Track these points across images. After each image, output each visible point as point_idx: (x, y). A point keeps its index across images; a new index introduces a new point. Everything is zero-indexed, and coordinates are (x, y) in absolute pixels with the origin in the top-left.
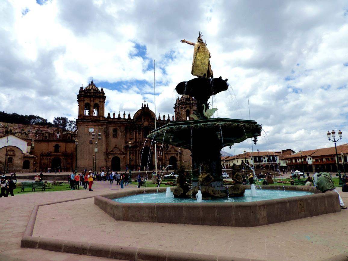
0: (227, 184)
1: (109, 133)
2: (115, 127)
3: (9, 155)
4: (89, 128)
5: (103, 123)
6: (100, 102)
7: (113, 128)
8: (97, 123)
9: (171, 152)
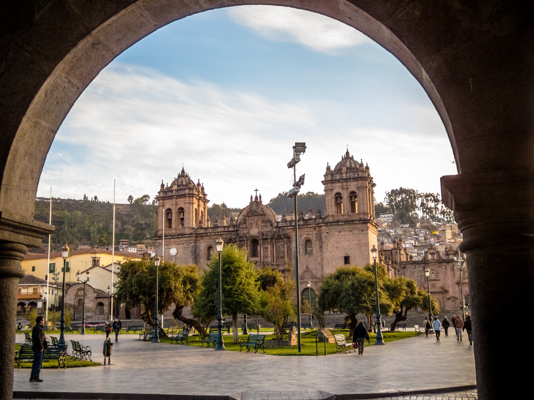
0: (148, 338)
1: (200, 254)
2: (208, 243)
3: (79, 296)
4: (169, 249)
5: (189, 238)
6: (185, 203)
7: (206, 244)
8: (181, 239)
9: (304, 279)
